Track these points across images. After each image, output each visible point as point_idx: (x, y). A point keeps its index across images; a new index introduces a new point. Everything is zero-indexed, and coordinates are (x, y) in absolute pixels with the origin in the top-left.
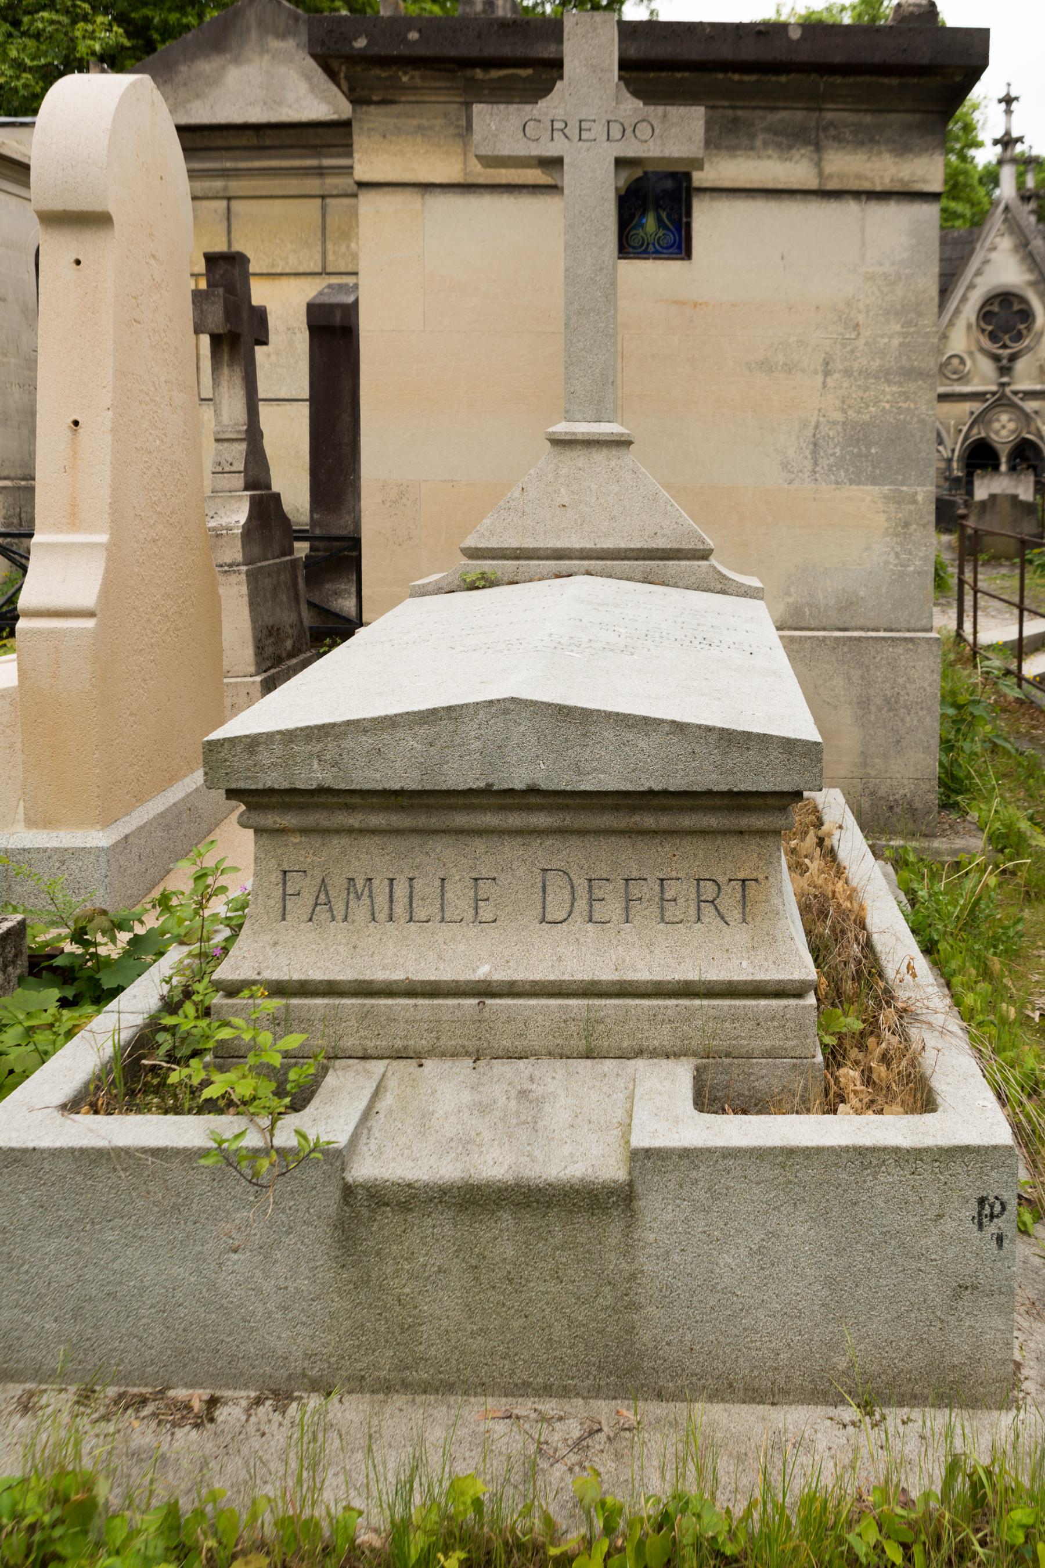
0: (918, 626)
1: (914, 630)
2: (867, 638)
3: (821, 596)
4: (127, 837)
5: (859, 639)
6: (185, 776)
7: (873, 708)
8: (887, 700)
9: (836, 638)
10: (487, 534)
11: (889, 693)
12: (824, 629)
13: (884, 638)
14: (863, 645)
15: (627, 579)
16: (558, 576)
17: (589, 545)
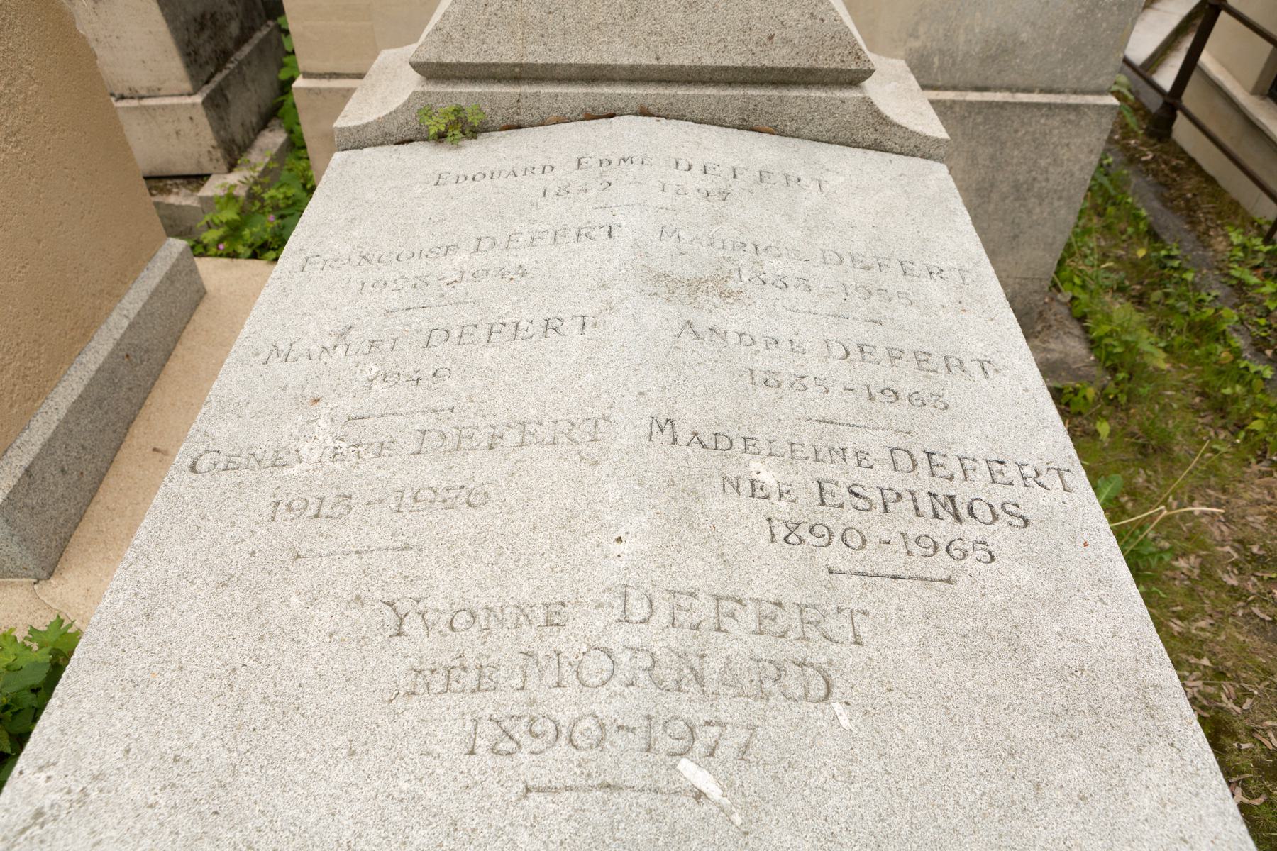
0: (1092, 85)
1: (1084, 92)
2: (1015, 104)
3: (962, 39)
4: (28, 472)
5: (1002, 105)
6: (108, 314)
7: (995, 196)
8: (1017, 187)
9: (971, 104)
10: (456, 35)
11: (1021, 178)
12: (955, 88)
13: (1038, 105)
14: (1005, 113)
15: (713, 123)
16: (590, 116)
17: (646, 60)
